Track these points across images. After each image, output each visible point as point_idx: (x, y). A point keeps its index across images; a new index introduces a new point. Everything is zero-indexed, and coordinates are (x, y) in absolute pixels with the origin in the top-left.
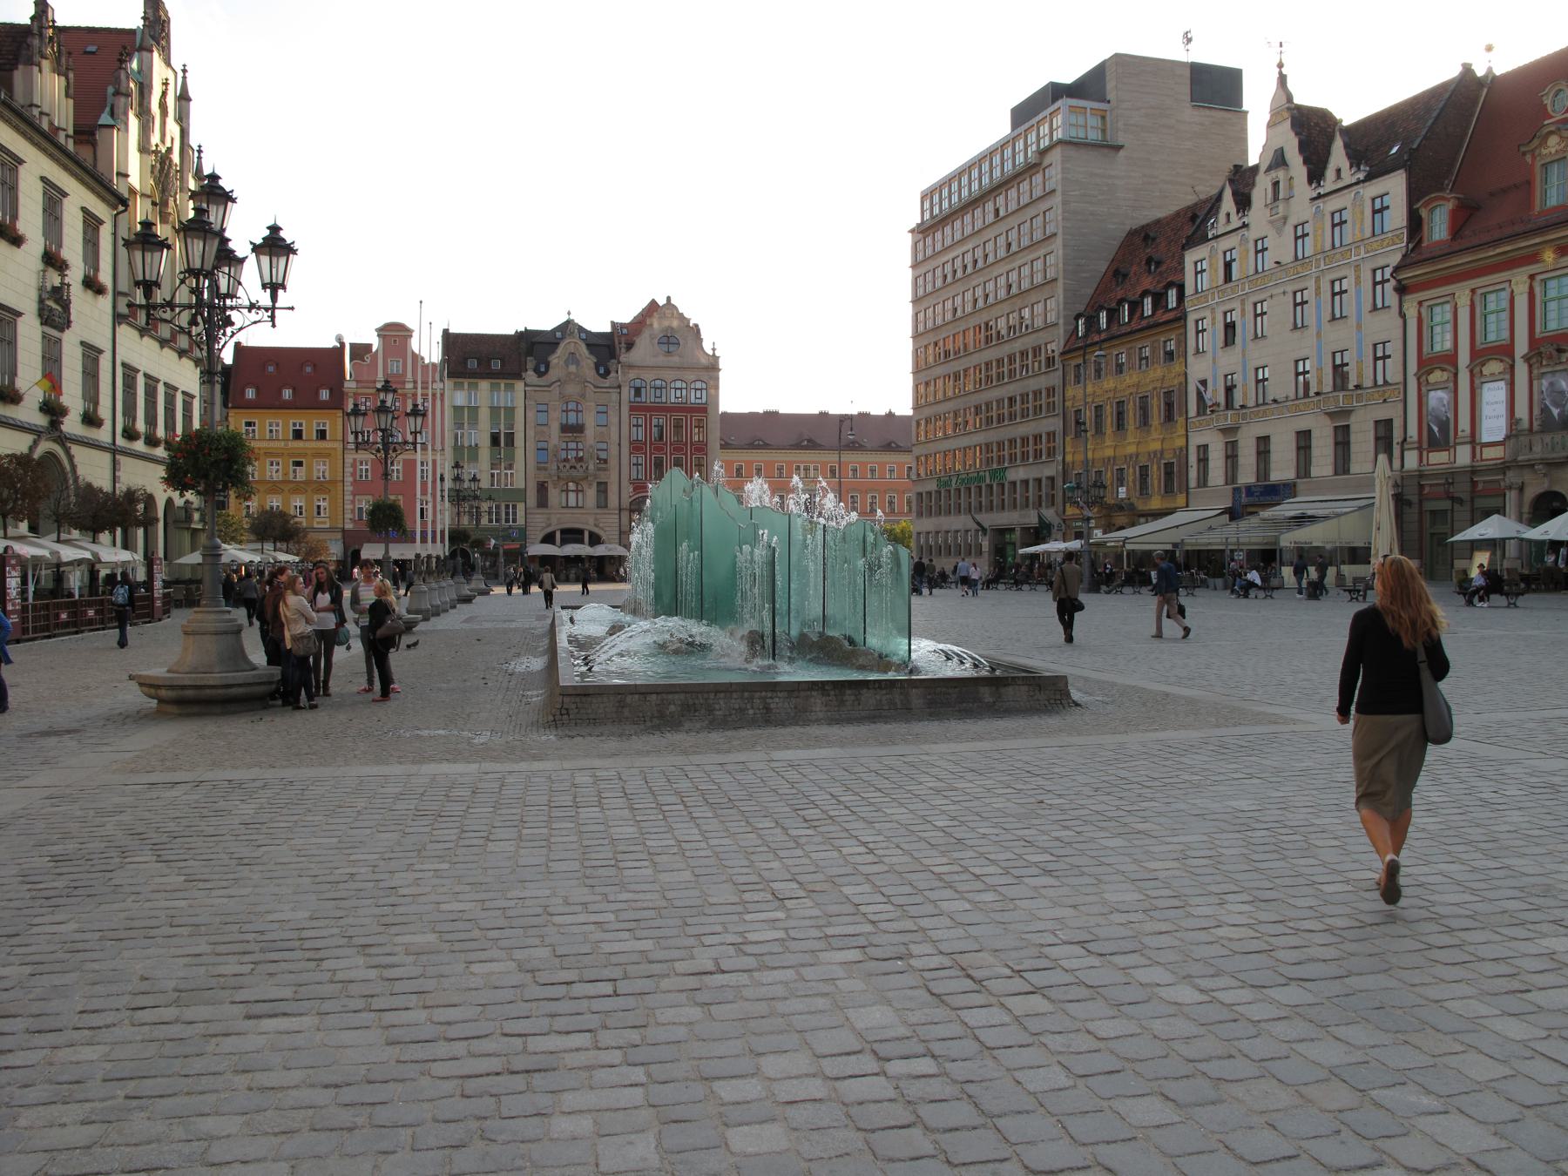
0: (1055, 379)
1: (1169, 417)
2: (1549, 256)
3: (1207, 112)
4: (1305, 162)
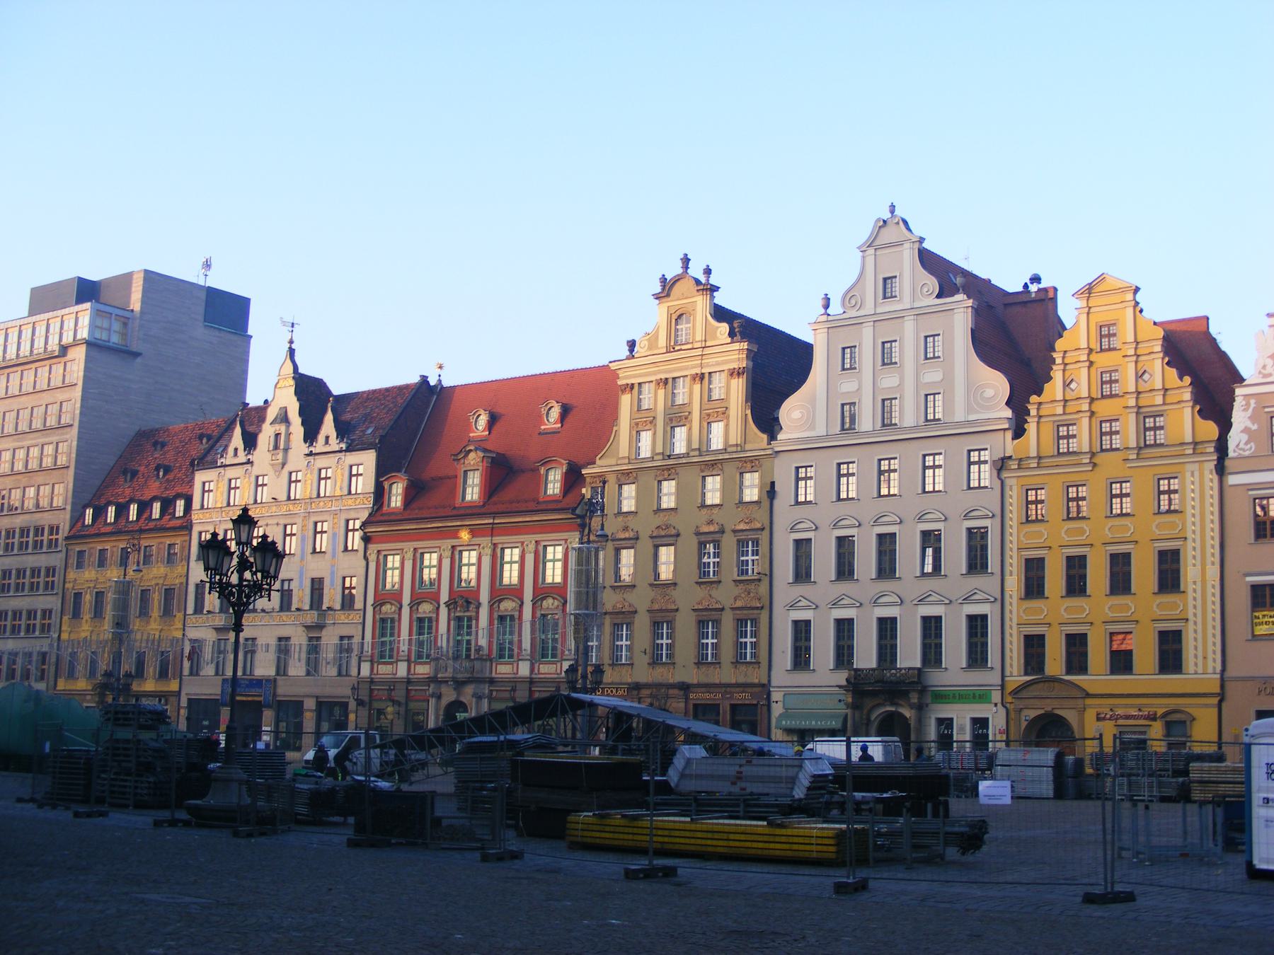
0: (56, 560)
1: (167, 612)
2: (465, 535)
3: (217, 333)
4: (303, 424)
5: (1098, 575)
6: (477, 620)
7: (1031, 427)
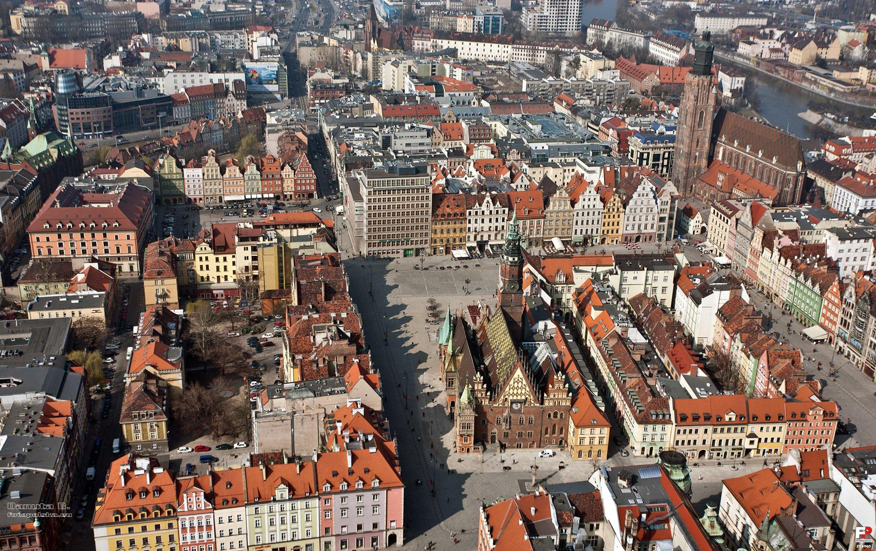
5: (611, 224)
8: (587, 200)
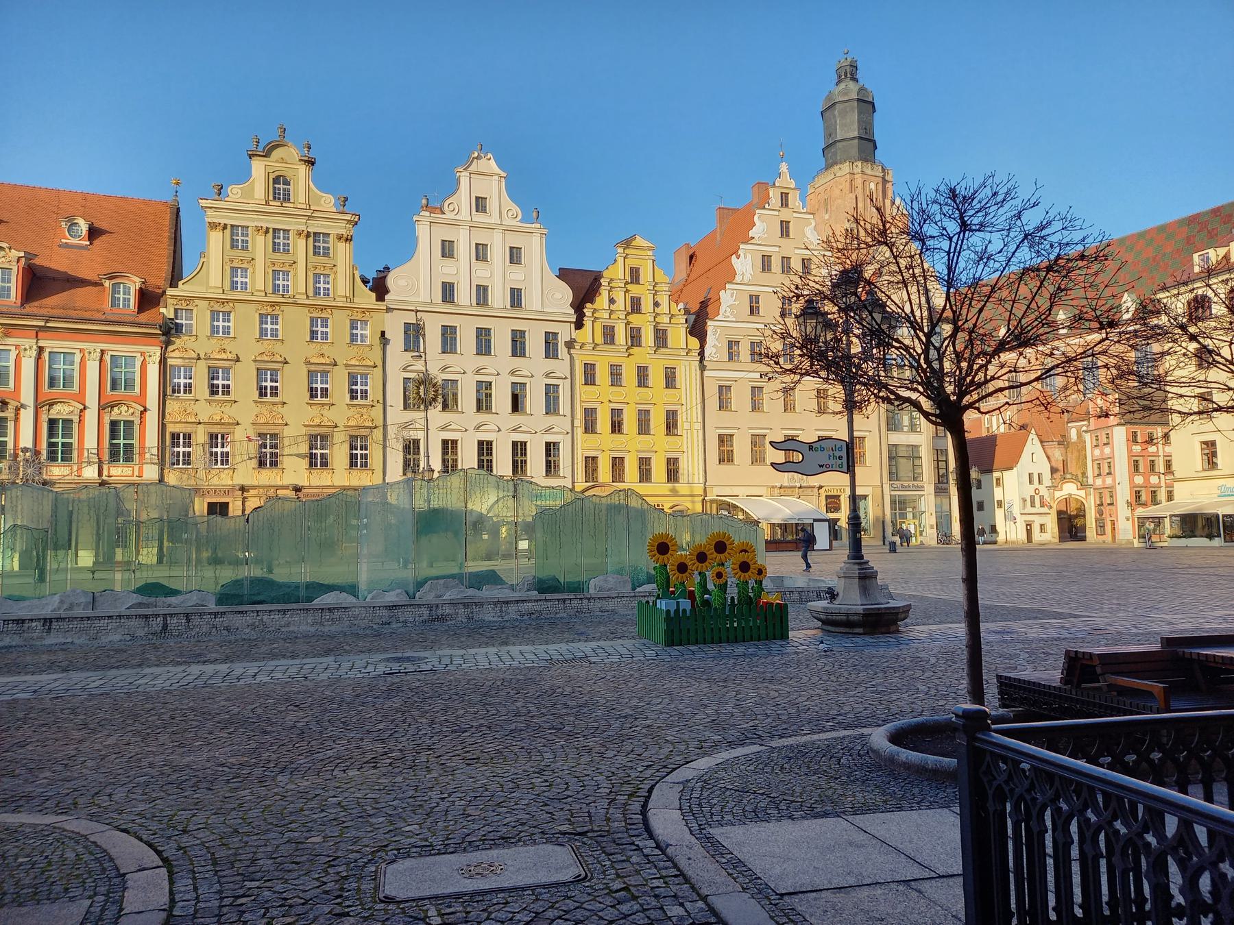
6: (17, 420)
7: (588, 322)
8: (464, 250)
